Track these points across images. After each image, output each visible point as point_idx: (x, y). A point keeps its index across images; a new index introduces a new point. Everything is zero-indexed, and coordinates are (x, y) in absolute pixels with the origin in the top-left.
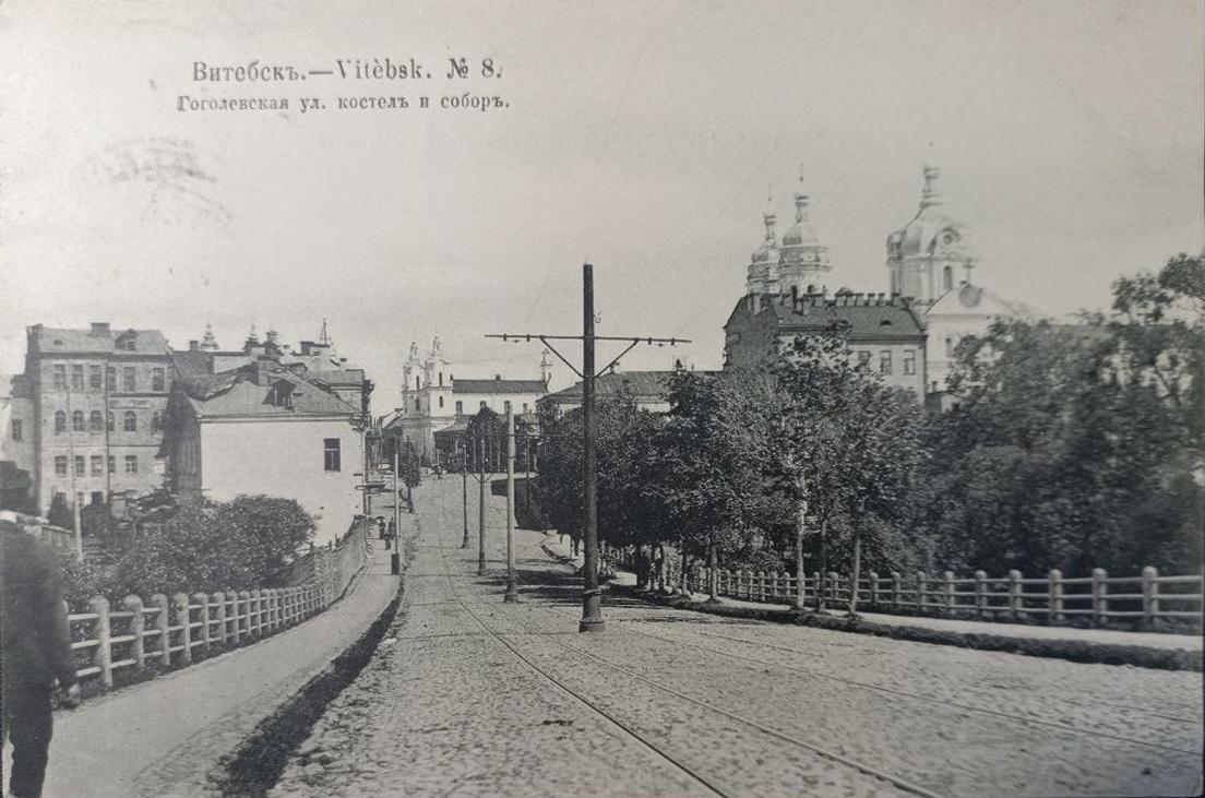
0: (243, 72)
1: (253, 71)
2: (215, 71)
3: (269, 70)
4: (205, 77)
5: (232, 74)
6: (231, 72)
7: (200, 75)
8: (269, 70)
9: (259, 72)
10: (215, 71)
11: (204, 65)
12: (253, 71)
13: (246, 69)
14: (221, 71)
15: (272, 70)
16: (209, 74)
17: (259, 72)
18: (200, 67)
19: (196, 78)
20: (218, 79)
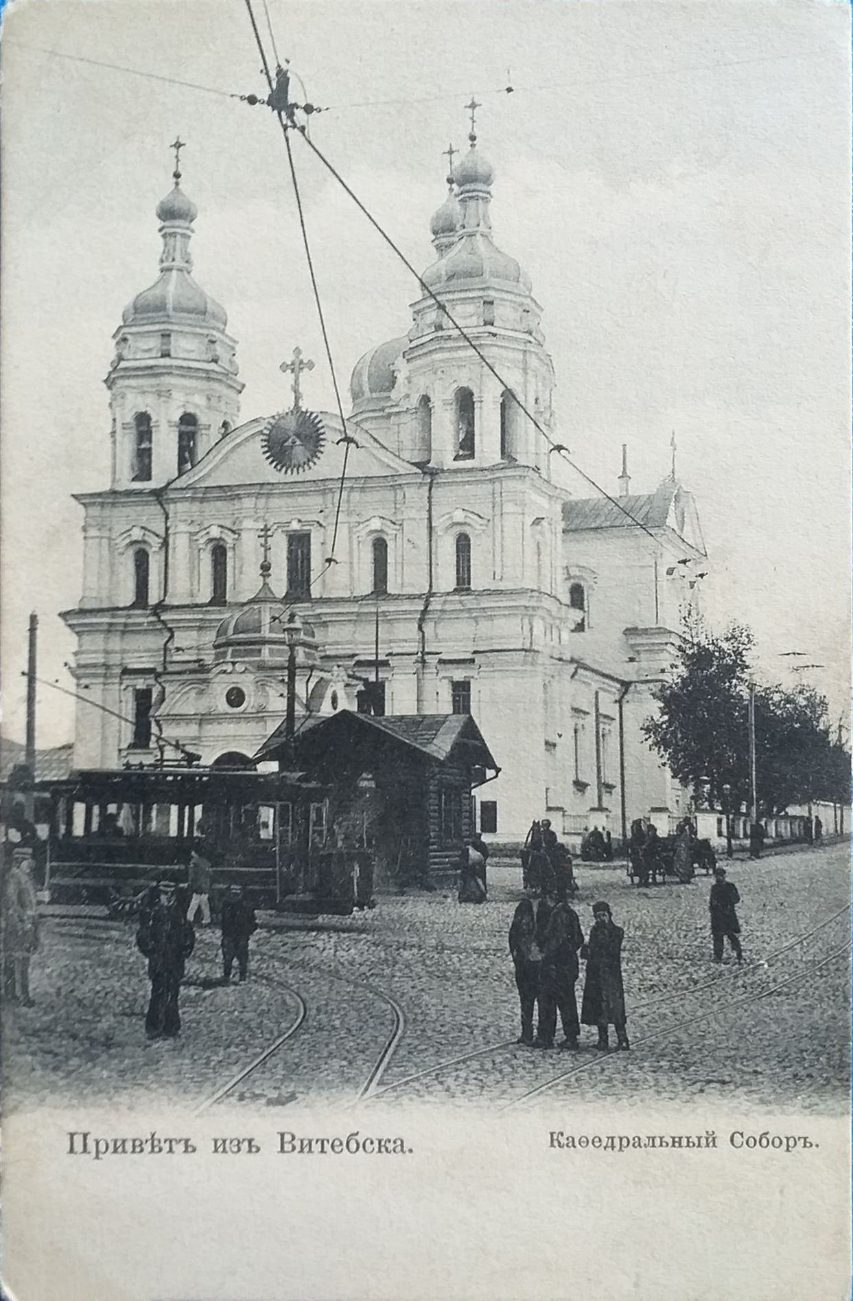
0: (341, 1144)
1: (353, 1146)
2: (306, 1142)
3: (372, 1143)
4: (294, 1148)
5: (327, 1147)
6: (325, 1142)
7: (288, 1147)
8: (372, 1143)
9: (361, 1148)
10: (306, 1142)
11: (293, 1138)
12: (353, 1146)
13: (345, 1144)
14: (313, 1143)
15: (376, 1143)
16: (297, 1144)
17: (361, 1148)
18: (288, 1138)
19: (282, 1150)
20: (310, 1151)
